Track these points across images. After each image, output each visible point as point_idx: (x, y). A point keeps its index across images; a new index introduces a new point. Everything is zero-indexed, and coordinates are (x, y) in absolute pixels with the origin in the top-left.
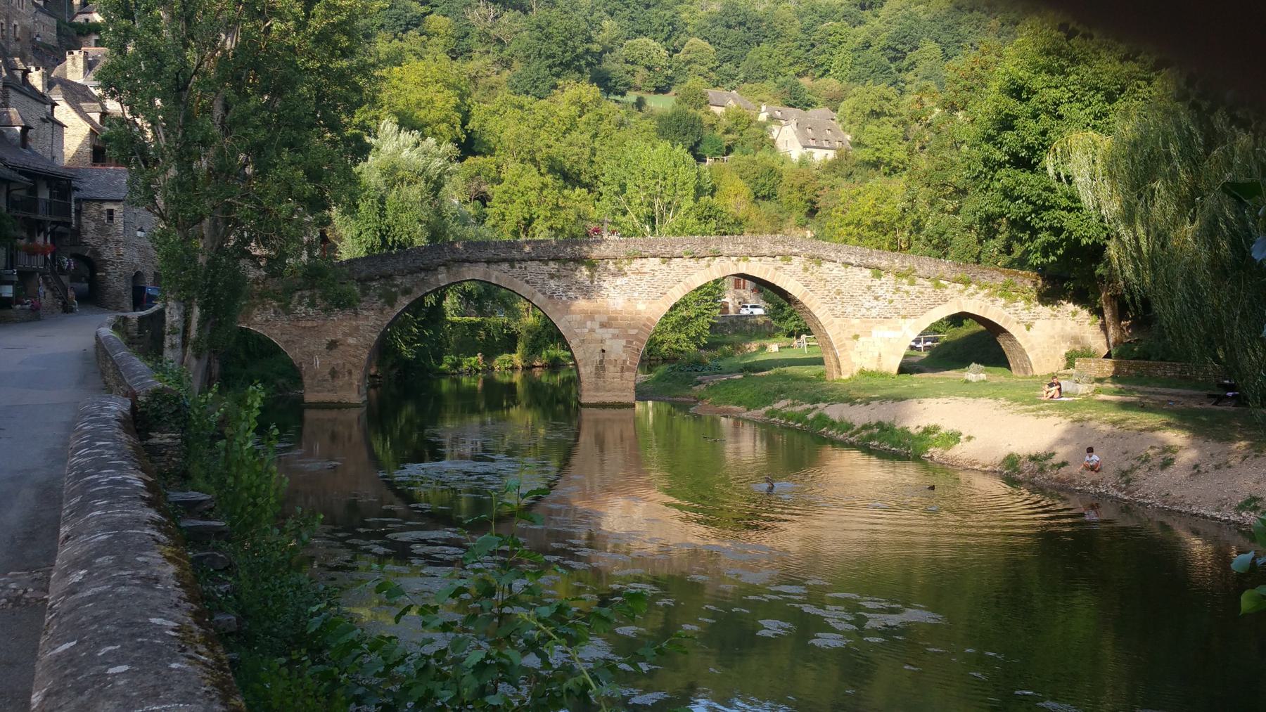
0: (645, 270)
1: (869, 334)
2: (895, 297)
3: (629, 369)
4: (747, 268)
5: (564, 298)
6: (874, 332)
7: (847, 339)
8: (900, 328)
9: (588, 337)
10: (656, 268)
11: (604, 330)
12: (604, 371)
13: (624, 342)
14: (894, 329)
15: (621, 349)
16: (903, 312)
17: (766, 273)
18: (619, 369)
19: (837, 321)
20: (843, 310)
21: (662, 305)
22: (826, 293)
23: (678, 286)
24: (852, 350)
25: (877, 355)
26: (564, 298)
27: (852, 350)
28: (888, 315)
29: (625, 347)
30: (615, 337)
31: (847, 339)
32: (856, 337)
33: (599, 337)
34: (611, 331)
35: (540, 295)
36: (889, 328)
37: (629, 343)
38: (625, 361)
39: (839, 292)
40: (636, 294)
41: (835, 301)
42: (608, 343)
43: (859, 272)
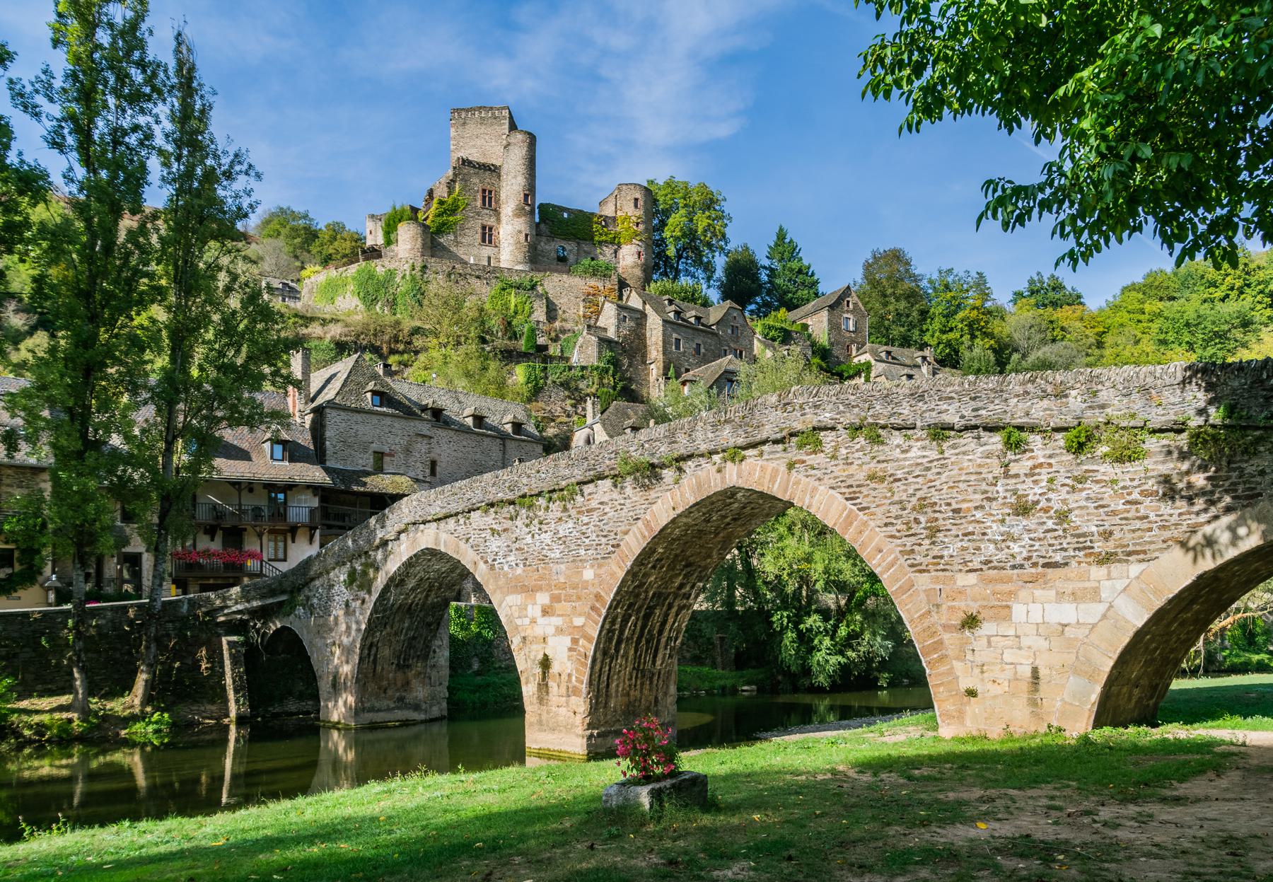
0: (594, 504)
1: (1003, 614)
2: (1076, 500)
3: (576, 692)
4: (739, 476)
5: (506, 568)
6: (1018, 610)
7: (946, 627)
8: (1095, 595)
9: (529, 632)
10: (605, 499)
11: (547, 620)
12: (547, 693)
13: (567, 641)
14: (1075, 597)
15: (565, 653)
16: (1099, 546)
17: (773, 480)
18: (563, 690)
19: (923, 581)
20: (936, 551)
21: (615, 568)
22: (895, 510)
23: (634, 528)
24: (961, 657)
25: (1027, 671)
26: (506, 568)
27: (961, 657)
28: (1058, 557)
29: (570, 649)
30: (560, 631)
31: (946, 627)
32: (971, 622)
33: (539, 631)
34: (556, 621)
35: (482, 566)
36: (1061, 596)
37: (575, 641)
38: (569, 675)
39: (923, 504)
40: (582, 552)
41: (916, 529)
42: (550, 640)
43: (973, 445)
